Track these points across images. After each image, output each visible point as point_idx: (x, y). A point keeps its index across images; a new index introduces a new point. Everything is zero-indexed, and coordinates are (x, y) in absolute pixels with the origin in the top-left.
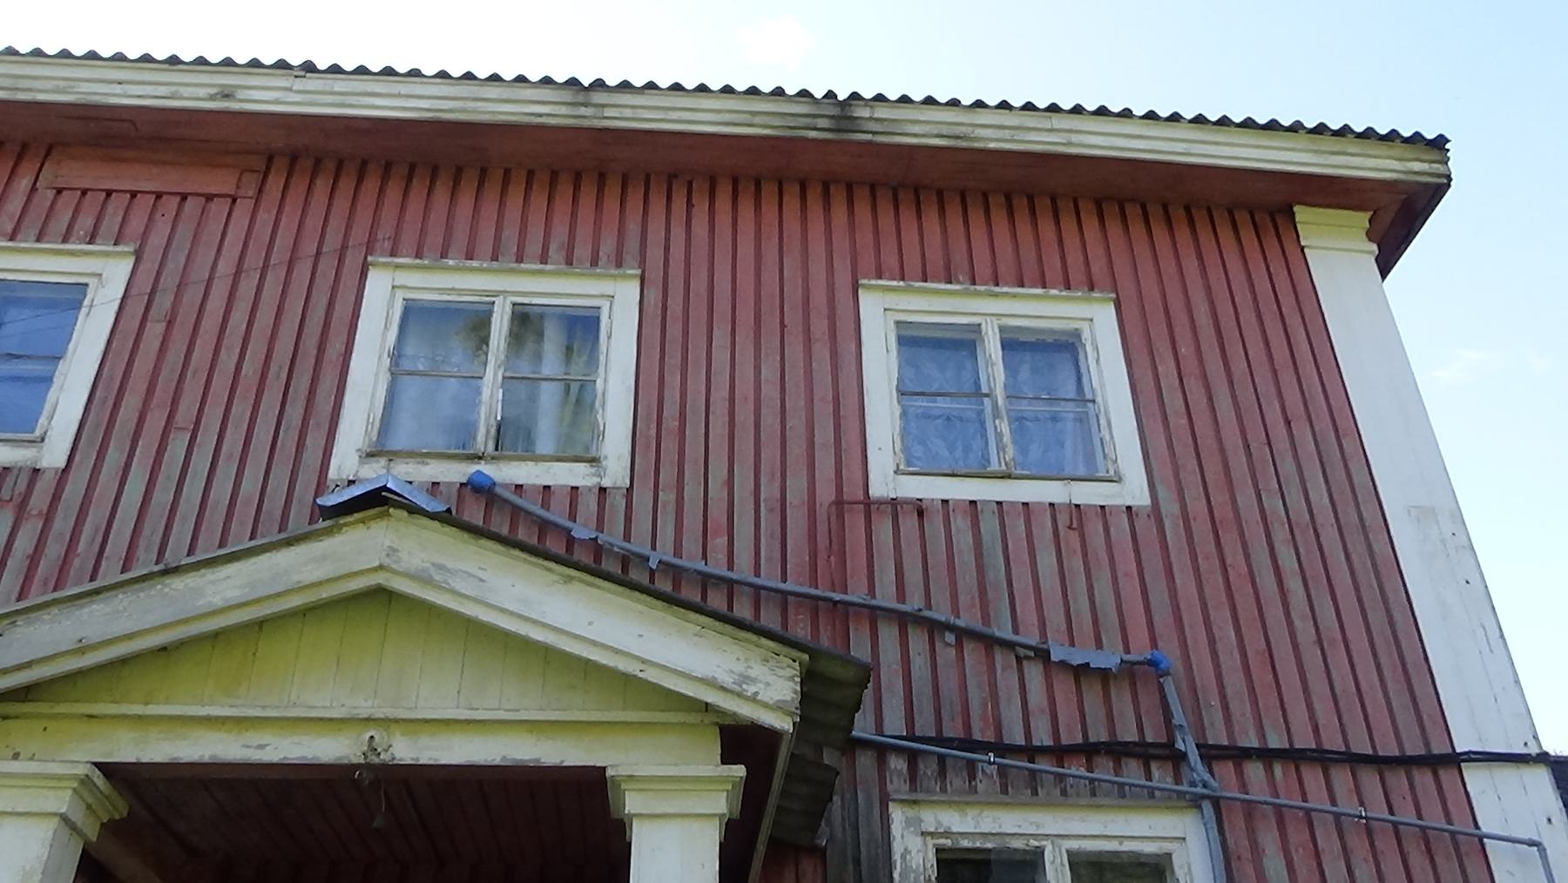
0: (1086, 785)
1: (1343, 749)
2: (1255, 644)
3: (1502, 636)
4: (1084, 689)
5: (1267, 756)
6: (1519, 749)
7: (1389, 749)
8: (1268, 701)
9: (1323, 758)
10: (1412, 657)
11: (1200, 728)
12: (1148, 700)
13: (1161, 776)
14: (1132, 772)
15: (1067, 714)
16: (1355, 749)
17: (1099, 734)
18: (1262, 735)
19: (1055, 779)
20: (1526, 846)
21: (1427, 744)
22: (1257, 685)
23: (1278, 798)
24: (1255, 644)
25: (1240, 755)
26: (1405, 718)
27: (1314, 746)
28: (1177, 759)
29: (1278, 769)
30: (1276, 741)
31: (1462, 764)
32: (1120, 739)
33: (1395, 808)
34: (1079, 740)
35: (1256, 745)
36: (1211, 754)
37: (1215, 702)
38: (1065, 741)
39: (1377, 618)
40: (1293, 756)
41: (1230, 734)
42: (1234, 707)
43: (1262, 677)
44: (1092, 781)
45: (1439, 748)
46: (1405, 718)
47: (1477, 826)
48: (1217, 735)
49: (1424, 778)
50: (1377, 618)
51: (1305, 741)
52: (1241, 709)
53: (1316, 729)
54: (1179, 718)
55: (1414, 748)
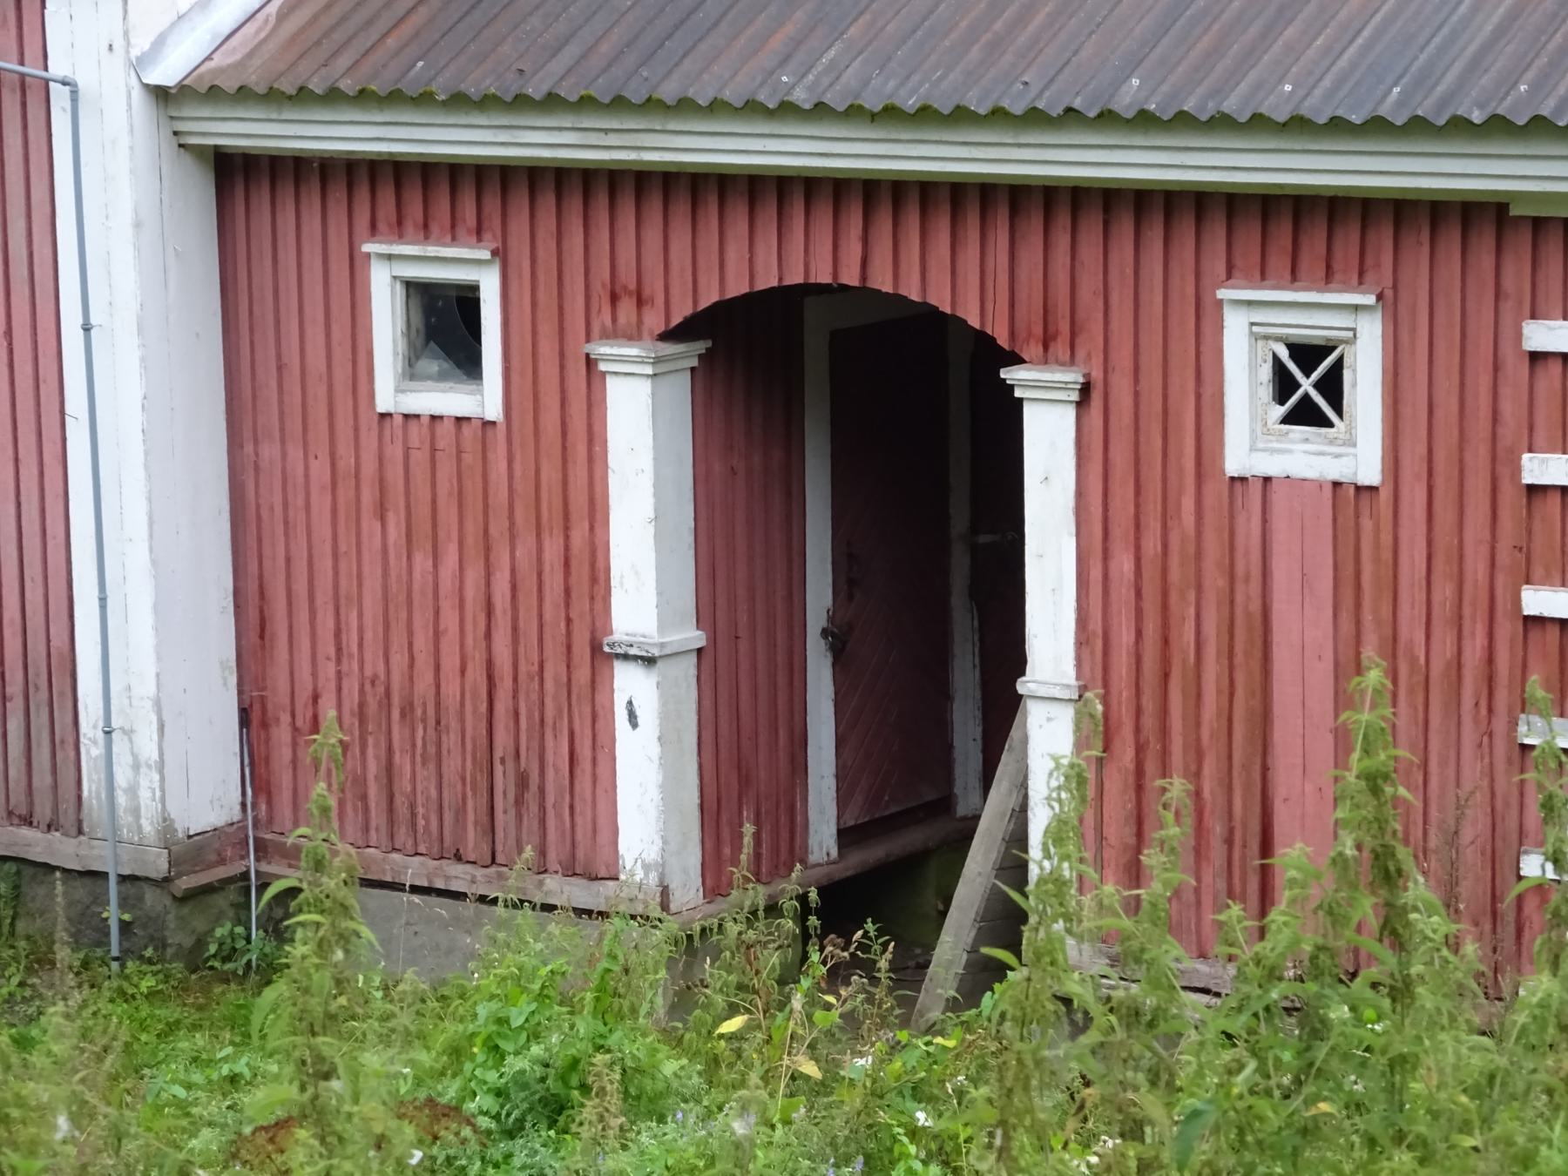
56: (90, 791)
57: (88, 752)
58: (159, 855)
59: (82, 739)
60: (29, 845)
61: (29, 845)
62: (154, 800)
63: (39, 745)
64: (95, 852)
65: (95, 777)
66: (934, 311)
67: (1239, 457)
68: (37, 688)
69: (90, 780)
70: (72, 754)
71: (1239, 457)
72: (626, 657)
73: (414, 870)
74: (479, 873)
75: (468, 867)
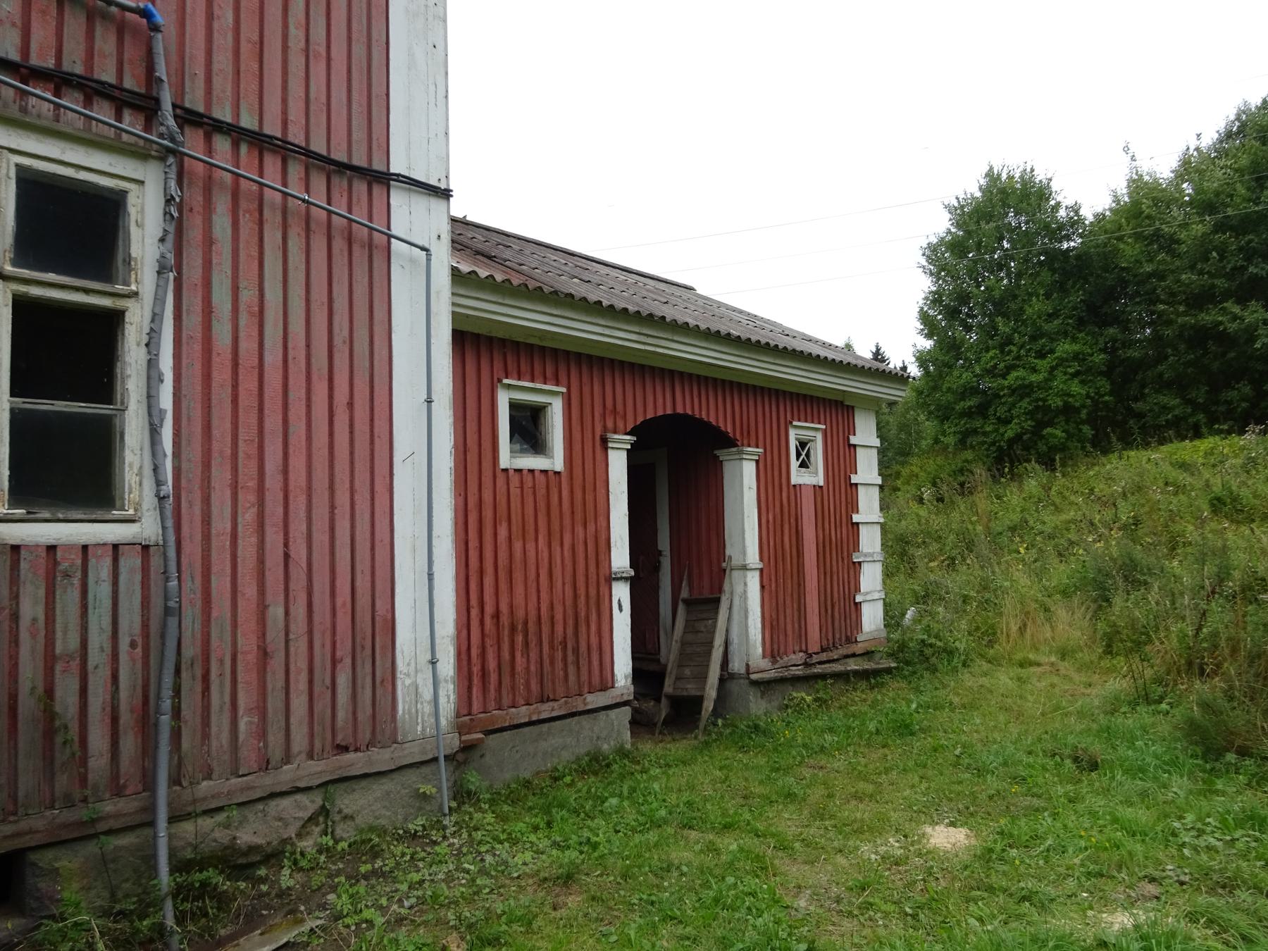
0: (49, 110)
1: (303, 144)
2: (249, 32)
3: (446, 97)
4: (66, 16)
5: (236, 133)
6: (433, 182)
7: (340, 155)
8: (249, 85)
9: (284, 149)
10: (377, 89)
11: (180, 90)
12: (132, 52)
13: (131, 123)
14: (103, 112)
15: (41, 34)
16: (313, 148)
17: (74, 64)
18: (237, 114)
19: (16, 94)
20: (419, 250)
21: (370, 160)
22: (243, 68)
23: (238, 168)
24: (249, 32)
25: (212, 127)
26: (359, 135)
27: (279, 135)
28: (147, 106)
29: (244, 149)
30: (248, 121)
31: (392, 183)
32: (96, 77)
33: (334, 201)
34: (50, 63)
35: (229, 119)
36: (188, 118)
37: (201, 72)
38: (34, 61)
39: (359, 50)
40: (259, 141)
41: (208, 103)
42: (217, 81)
43: (249, 64)
44: (58, 106)
45: (378, 166)
46: (359, 135)
47: (389, 228)
48: (195, 101)
49: (360, 187)
50: (359, 50)
51: (272, 128)
52: (222, 85)
53: (285, 123)
54: (161, 71)
55: (359, 160)
56: (404, 711)
57: (403, 683)
58: (453, 738)
59: (399, 675)
60: (352, 765)
61: (352, 765)
62: (448, 702)
63: (363, 688)
64: (406, 752)
65: (407, 699)
66: (708, 424)
67: (794, 480)
68: (363, 647)
69: (404, 702)
70: (390, 688)
71: (794, 480)
72: (617, 579)
73: (523, 713)
74: (555, 704)
75: (551, 704)
